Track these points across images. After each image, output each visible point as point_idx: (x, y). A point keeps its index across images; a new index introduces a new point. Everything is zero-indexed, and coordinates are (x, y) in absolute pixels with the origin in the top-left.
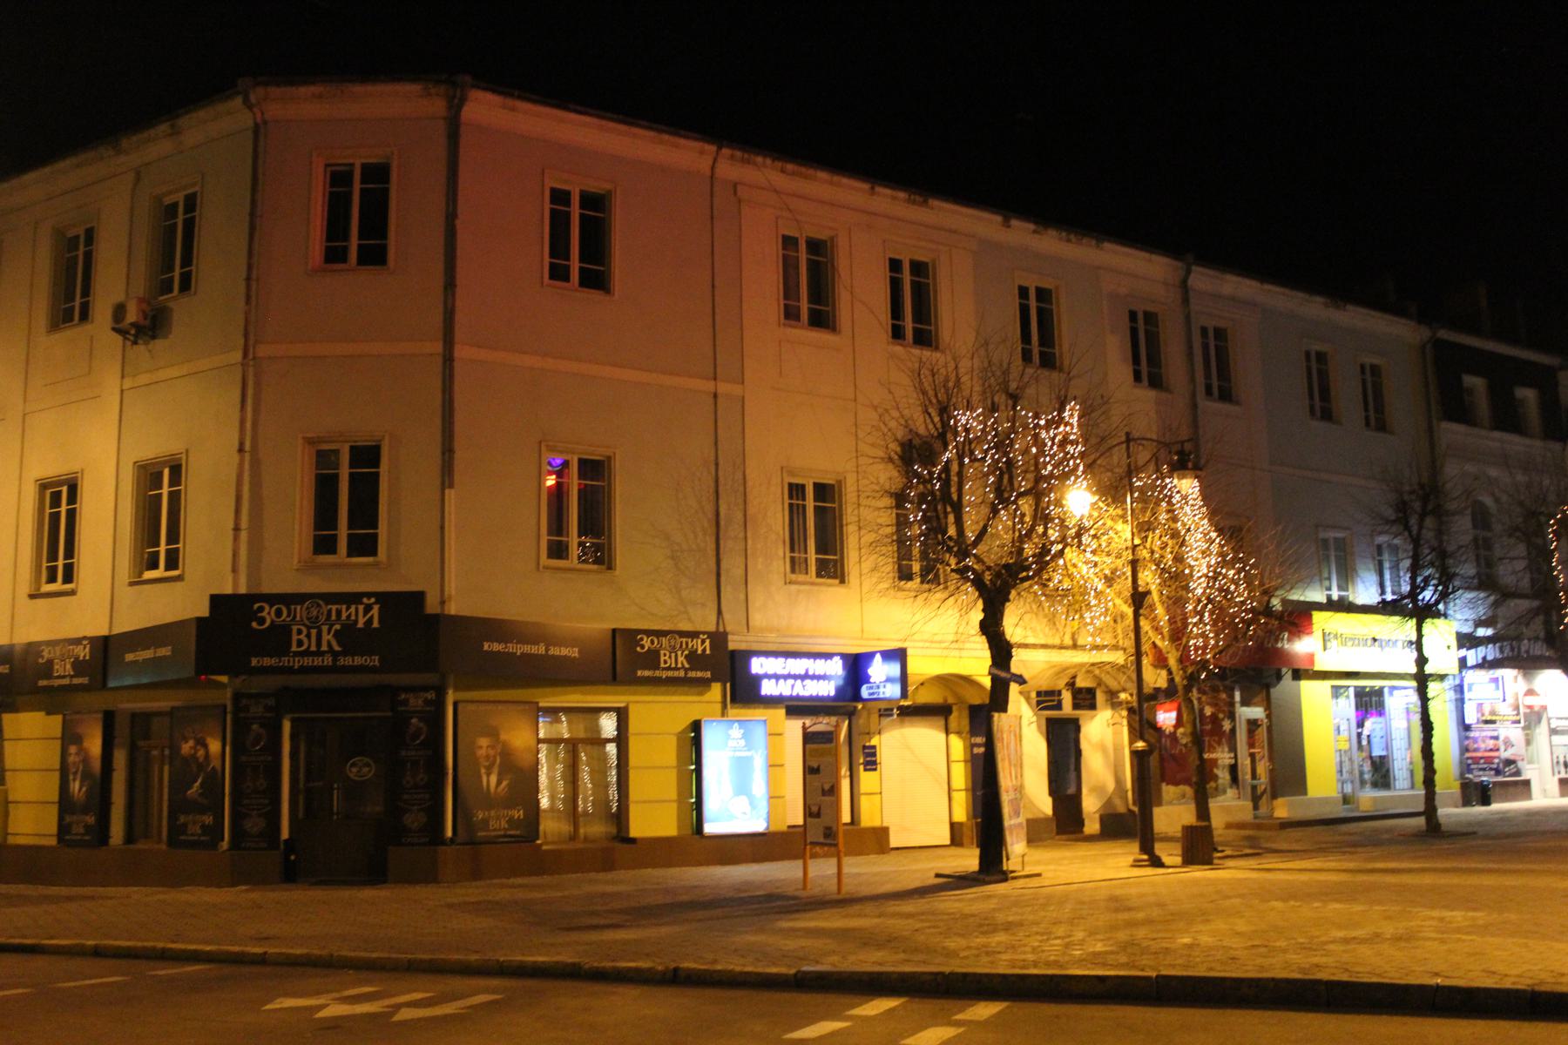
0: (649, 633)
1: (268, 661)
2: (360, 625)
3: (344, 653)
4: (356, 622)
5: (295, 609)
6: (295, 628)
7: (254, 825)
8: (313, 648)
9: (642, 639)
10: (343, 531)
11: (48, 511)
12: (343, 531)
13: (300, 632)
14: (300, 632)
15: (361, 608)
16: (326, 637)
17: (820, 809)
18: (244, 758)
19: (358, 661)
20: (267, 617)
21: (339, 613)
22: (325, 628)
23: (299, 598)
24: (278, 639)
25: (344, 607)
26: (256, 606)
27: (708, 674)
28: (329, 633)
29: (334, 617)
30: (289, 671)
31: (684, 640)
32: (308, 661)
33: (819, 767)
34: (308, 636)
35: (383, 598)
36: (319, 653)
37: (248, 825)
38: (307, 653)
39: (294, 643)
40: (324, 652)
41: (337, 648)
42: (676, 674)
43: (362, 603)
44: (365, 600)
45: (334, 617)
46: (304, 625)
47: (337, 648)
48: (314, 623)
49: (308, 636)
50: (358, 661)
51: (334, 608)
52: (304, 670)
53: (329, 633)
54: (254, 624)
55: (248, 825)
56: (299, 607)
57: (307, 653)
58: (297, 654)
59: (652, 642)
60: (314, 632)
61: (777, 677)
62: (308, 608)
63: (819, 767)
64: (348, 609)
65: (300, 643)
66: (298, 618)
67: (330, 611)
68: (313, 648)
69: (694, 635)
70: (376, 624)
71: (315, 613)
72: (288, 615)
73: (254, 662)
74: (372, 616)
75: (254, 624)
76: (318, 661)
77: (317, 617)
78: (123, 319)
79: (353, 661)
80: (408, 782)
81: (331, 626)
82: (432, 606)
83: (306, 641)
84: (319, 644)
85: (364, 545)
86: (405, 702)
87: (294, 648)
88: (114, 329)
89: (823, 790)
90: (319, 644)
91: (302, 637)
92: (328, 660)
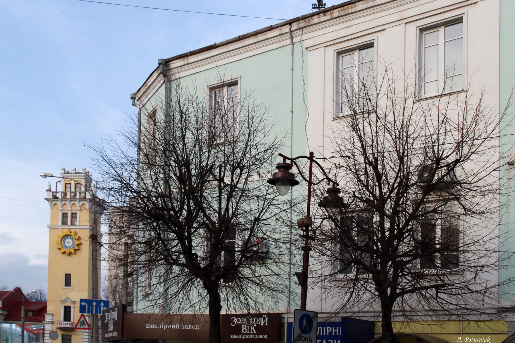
2: (262, 325)
3: (257, 334)
4: (261, 323)
6: (243, 325)
13: (244, 327)
14: (244, 327)
15: (262, 319)
22: (252, 326)
24: (238, 329)
35: (269, 315)
36: (250, 334)
38: (246, 334)
39: (243, 331)
41: (255, 332)
46: (246, 324)
47: (255, 332)
49: (247, 328)
54: (232, 324)
57: (246, 334)
58: (244, 334)
60: (249, 327)
64: (259, 319)
65: (245, 330)
67: (253, 320)
70: (266, 325)
72: (241, 321)
75: (232, 324)
76: (249, 337)
81: (254, 325)
83: (246, 329)
84: (250, 331)
90: (250, 331)
91: (245, 328)
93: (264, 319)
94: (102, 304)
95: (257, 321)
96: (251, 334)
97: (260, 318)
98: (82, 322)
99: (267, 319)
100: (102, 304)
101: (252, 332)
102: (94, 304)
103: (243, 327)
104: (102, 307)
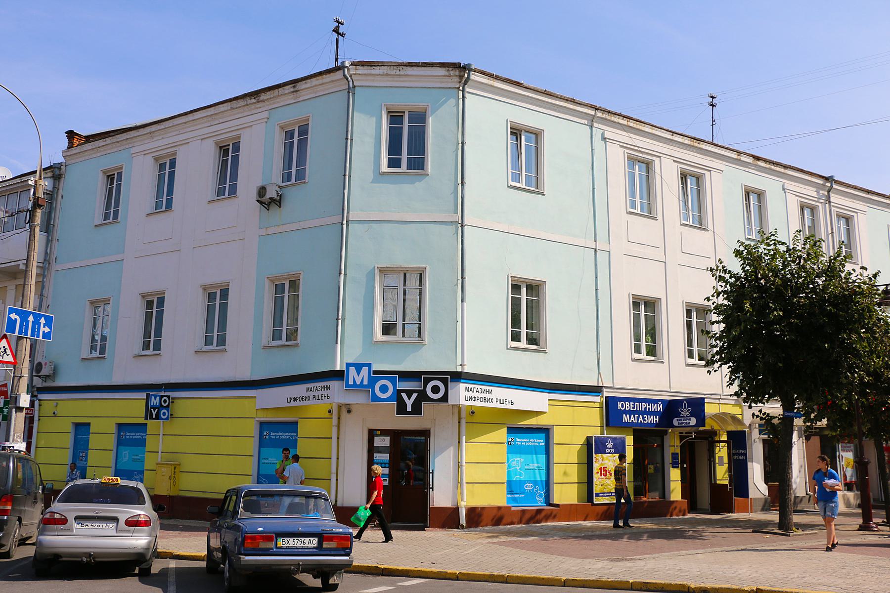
61: (630, 413)
88: (258, 201)
94: (43, 321)
100: (43, 321)
102: (31, 318)
104: (42, 325)
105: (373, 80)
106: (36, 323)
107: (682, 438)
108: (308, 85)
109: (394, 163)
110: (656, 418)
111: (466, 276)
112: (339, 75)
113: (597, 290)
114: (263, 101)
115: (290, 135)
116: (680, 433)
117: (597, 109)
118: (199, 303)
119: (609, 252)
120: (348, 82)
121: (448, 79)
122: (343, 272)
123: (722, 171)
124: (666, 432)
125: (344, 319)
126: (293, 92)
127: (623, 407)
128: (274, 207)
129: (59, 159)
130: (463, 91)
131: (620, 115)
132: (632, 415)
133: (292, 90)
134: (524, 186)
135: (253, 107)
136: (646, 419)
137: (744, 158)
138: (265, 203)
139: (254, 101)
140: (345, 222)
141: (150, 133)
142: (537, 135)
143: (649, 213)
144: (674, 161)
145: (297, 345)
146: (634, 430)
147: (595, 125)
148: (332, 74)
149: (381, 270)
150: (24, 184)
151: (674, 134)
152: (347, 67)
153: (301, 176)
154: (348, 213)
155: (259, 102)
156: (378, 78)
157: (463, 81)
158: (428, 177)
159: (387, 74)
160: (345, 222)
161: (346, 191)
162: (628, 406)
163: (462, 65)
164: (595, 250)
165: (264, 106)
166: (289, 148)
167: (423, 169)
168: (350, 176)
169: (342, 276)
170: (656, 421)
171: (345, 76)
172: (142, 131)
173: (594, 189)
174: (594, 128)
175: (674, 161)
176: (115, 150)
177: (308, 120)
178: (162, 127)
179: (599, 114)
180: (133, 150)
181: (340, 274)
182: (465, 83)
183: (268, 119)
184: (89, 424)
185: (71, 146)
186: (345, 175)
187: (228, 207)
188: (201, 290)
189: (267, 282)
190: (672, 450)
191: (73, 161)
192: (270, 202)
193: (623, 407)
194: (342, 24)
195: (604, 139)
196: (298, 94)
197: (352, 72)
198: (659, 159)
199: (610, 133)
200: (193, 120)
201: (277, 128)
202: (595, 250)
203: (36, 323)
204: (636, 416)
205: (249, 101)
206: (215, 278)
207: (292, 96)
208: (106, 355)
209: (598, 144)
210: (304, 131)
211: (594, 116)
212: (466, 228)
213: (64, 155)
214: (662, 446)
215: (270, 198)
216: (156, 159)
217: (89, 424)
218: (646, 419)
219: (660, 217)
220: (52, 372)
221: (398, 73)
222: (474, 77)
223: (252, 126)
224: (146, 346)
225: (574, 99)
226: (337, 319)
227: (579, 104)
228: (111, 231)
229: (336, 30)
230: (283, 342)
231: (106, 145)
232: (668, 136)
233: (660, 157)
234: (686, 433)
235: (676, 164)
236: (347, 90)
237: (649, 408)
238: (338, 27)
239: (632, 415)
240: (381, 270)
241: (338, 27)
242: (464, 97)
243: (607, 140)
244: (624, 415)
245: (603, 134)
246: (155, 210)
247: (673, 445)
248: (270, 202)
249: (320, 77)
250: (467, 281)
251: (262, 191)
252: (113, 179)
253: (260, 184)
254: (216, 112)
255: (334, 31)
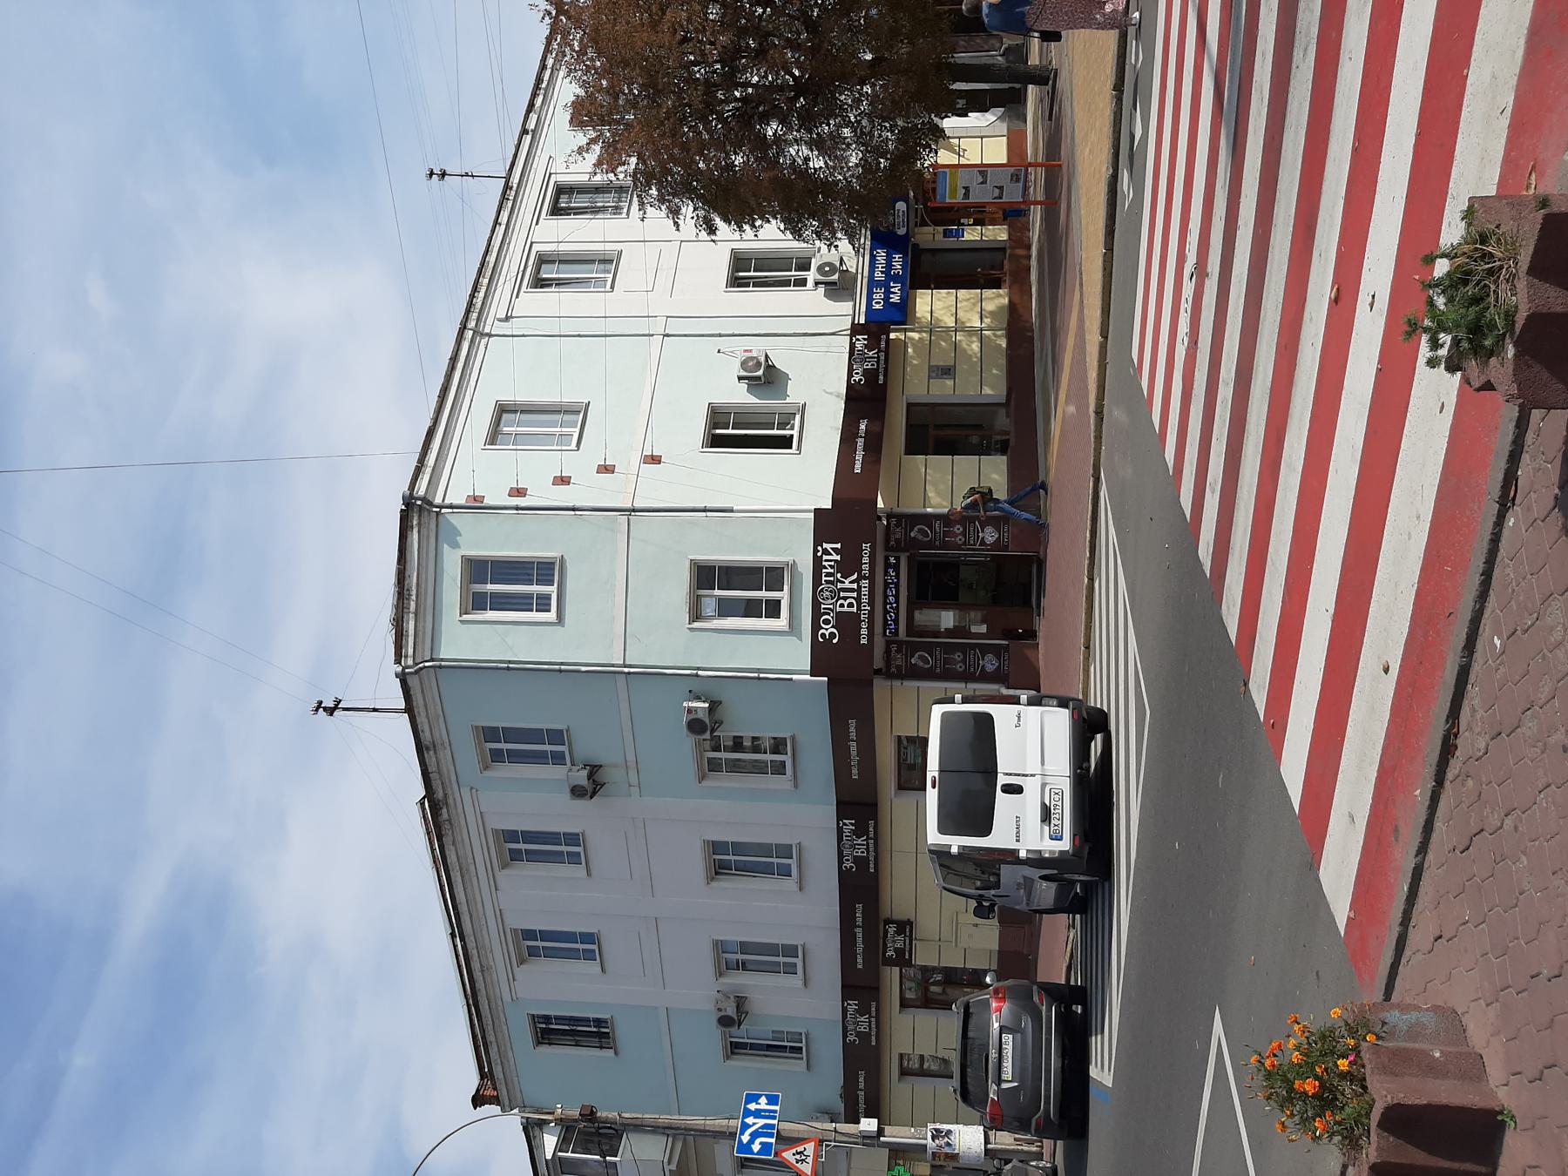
0: (850, 375)
1: (864, 632)
2: (838, 558)
4: (835, 561)
5: (824, 609)
6: (838, 609)
7: (990, 663)
8: (855, 595)
9: (854, 380)
10: (763, 594)
11: (734, 872)
12: (763, 594)
13: (842, 606)
15: (825, 557)
16: (847, 585)
17: (996, 187)
18: (937, 543)
19: (866, 560)
20: (829, 631)
21: (828, 575)
23: (816, 604)
24: (847, 623)
25: (824, 571)
26: (821, 640)
27: (884, 337)
28: (844, 583)
29: (832, 579)
30: (871, 614)
31: (856, 352)
32: (865, 599)
33: (964, 187)
34: (845, 598)
35: (818, 542)
36: (859, 590)
37: (990, 668)
38: (858, 599)
39: (851, 610)
40: (858, 585)
41: (855, 576)
42: (882, 358)
43: (822, 556)
44: (819, 554)
45: (832, 579)
46: (837, 601)
47: (855, 576)
48: (836, 595)
49: (845, 598)
50: (866, 560)
51: (824, 578)
52: (871, 603)
53: (844, 583)
54: (835, 641)
55: (990, 668)
56: (823, 606)
57: (858, 599)
58: (859, 608)
59: (857, 373)
60: (842, 594)
62: (823, 599)
63: (964, 187)
65: (850, 605)
66: (831, 606)
68: (855, 595)
69: (852, 346)
70: (839, 546)
71: (827, 593)
72: (829, 614)
73: (863, 641)
74: (831, 548)
75: (835, 641)
76: (865, 591)
77: (831, 592)
78: (582, 787)
79: (866, 563)
80: (960, 667)
82: (827, 504)
83: (848, 601)
84: (852, 590)
85: (773, 576)
86: (898, 541)
87: (855, 610)
88: (591, 798)
89: (982, 183)
90: (852, 590)
92: (865, 583)
93: (826, 552)
95: (832, 571)
96: (859, 587)
97: (824, 563)
98: (798, 1157)
99: (825, 545)
101: (855, 586)
103: (842, 609)
105: (424, 632)
106: (758, 1114)
107: (924, 224)
108: (426, 728)
109: (543, 604)
110: (895, 258)
111: (702, 505)
112: (413, 682)
113: (720, 335)
114: (445, 795)
115: (497, 756)
116: (916, 225)
117: (465, 327)
118: (730, 885)
119: (667, 317)
120: (425, 667)
121: (424, 531)
122: (695, 672)
123: (550, 157)
124: (916, 246)
125: (759, 671)
126: (435, 753)
127: (880, 303)
128: (599, 777)
129: (514, 1121)
130: (441, 507)
131: (472, 296)
132: (892, 290)
133: (432, 753)
134: (577, 430)
135: (453, 812)
136: (896, 272)
137: (531, 125)
138: (595, 789)
139: (444, 810)
140: (626, 670)
141: (482, 971)
142: (502, 410)
143: (608, 261)
144: (537, 224)
145: (793, 738)
146: (910, 288)
147: (487, 330)
148: (412, 692)
149: (692, 621)
150: (551, 1166)
151: (499, 221)
152: (404, 669)
153: (556, 736)
154: (613, 666)
155: (447, 803)
156: (420, 627)
157: (428, 507)
158: (564, 556)
159: (416, 614)
160: (626, 670)
161: (583, 669)
162: (879, 295)
163: (403, 507)
164: (664, 336)
165: (453, 794)
166: (517, 757)
167: (553, 563)
168: (562, 664)
169: (700, 673)
170: (899, 258)
171: (416, 672)
172: (480, 985)
173: (579, 336)
174: (493, 333)
175: (537, 224)
176: (505, 1027)
177: (477, 727)
178: (475, 951)
179: (472, 324)
180: (507, 998)
181: (697, 675)
182: (431, 504)
183: (472, 788)
184: (901, 1056)
185: (495, 1100)
186: (560, 671)
187: (601, 845)
188: (714, 884)
189: (705, 783)
190: (939, 237)
191: (519, 1095)
192: (594, 781)
193: (880, 303)
194: (320, 703)
195: (507, 319)
196: (438, 742)
197: (410, 662)
198: (534, 245)
199: (498, 307)
200: (468, 905)
201: (488, 773)
202: (664, 336)
203: (758, 1114)
204: (892, 285)
205: (445, 815)
206: (697, 864)
207: (441, 755)
208: (803, 1031)
209: (514, 327)
210: (490, 734)
211: (474, 332)
212: (637, 505)
213: (507, 1108)
214: (934, 251)
215: (589, 780)
216: (522, 961)
217: (901, 1056)
218: (896, 272)
219: (618, 247)
220: (826, 1116)
221: (414, 597)
222: (421, 489)
223: (481, 813)
224: (790, 970)
225: (451, 359)
226: (759, 678)
227: (458, 350)
228: (623, 1032)
229: (331, 711)
230: (787, 759)
231: (497, 1042)
232: (500, 230)
233: (532, 243)
234: (916, 217)
235: (541, 219)
236: (437, 669)
237: (882, 267)
238: (325, 709)
239: (892, 290)
240: (692, 621)
241: (325, 709)
242: (451, 506)
243: (509, 314)
244: (891, 300)
245: (500, 320)
246: (595, 960)
247: (930, 236)
248: (594, 781)
249: (416, 710)
250: (709, 505)
251: (577, 792)
252: (548, 1031)
253: (568, 795)
254: (458, 868)
255: (331, 715)
